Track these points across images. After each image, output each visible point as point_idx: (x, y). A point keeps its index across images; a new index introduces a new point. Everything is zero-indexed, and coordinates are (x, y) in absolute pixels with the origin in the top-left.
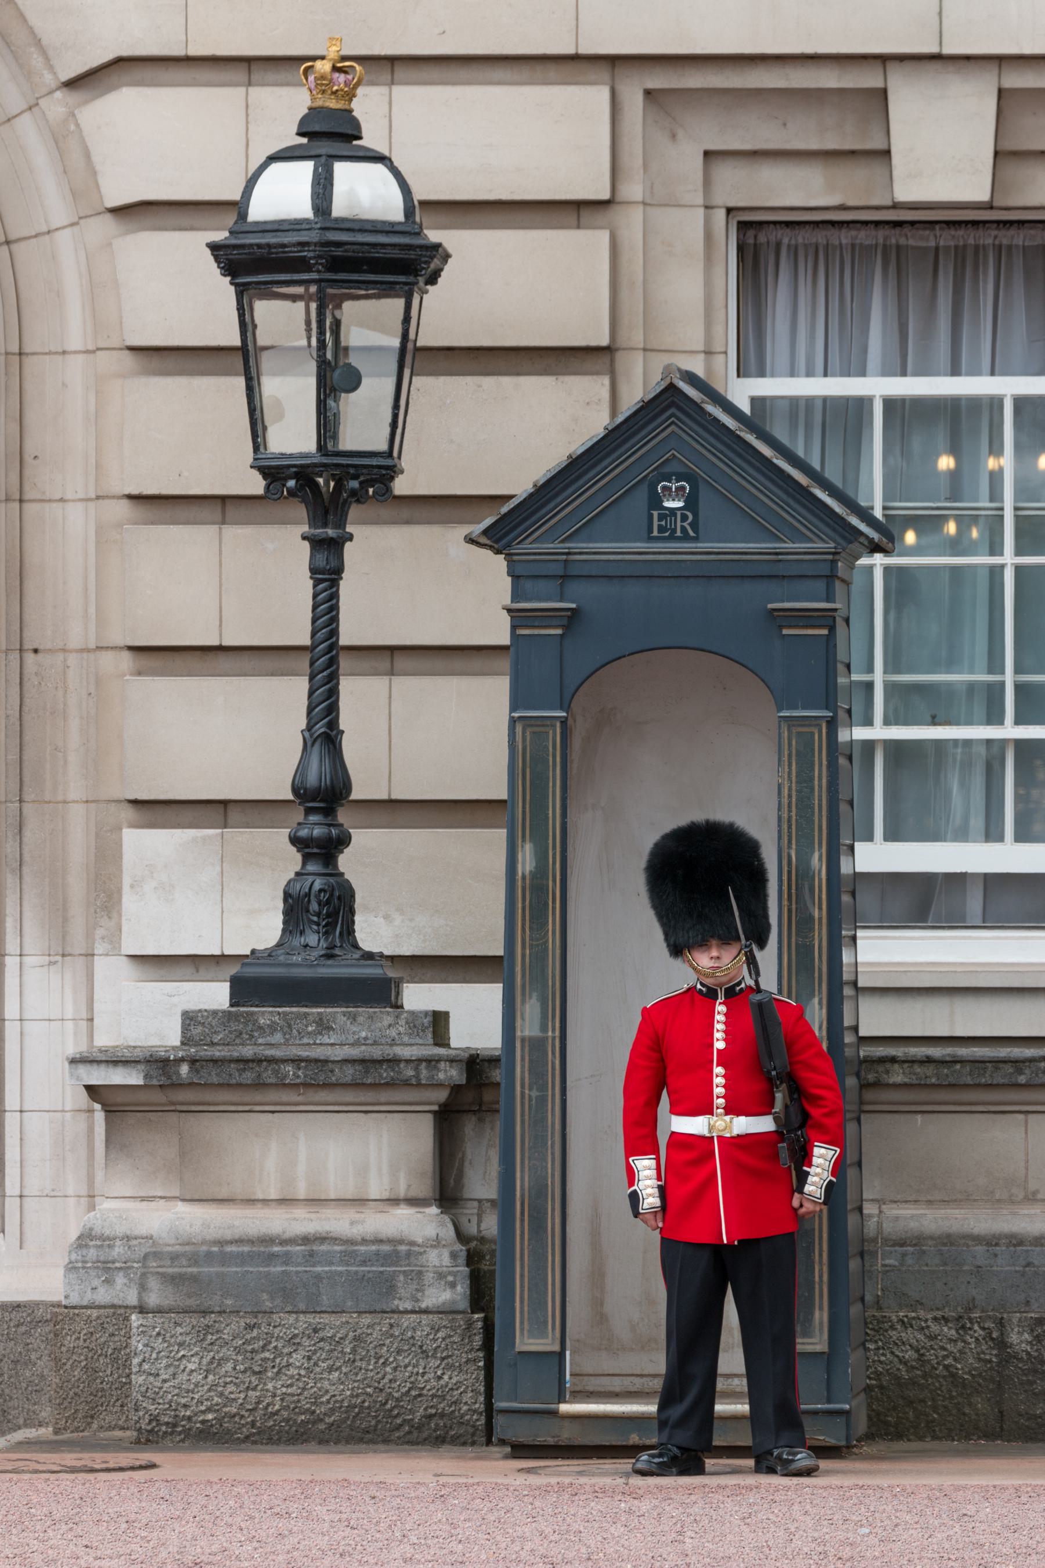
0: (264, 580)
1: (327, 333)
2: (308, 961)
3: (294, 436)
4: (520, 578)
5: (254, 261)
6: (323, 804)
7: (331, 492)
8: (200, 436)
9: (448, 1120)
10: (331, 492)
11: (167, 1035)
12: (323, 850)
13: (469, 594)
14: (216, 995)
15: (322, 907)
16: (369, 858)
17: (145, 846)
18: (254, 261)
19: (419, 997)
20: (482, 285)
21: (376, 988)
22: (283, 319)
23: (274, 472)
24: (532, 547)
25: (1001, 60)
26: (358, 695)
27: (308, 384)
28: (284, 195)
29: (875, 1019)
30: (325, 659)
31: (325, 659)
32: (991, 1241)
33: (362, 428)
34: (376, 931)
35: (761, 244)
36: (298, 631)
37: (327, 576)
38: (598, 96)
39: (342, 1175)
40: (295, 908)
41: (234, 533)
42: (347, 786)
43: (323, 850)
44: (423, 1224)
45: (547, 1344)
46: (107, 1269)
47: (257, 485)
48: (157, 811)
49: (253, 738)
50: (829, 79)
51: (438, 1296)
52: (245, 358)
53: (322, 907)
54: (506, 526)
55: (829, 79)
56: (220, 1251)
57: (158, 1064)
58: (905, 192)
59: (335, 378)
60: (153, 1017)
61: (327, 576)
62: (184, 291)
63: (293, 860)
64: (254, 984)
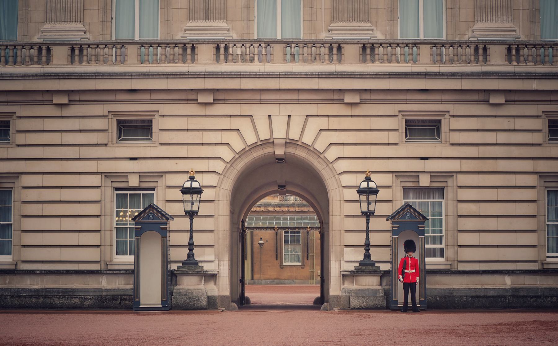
0: (361, 223)
1: (368, 198)
2: (367, 261)
3: (365, 209)
4: (393, 223)
5: (361, 192)
6: (367, 246)
7: (368, 215)
8: (355, 209)
9: (381, 277)
10: (368, 215)
11: (353, 269)
12: (367, 250)
13: (387, 225)
14: (358, 265)
15: (367, 256)
16: (372, 251)
17: (347, 250)
18: (361, 192)
19: (377, 265)
20: (382, 194)
21: (373, 263)
22: (364, 198)
23: (363, 213)
24: (394, 220)
25: (430, 172)
26: (371, 235)
27: (366, 204)
28: (364, 185)
29: (427, 267)
30: (368, 231)
31: (368, 231)
32: (435, 289)
33: (371, 208)
34: (373, 258)
35: (406, 190)
36: (365, 228)
37: (368, 223)
38: (391, 175)
39: (370, 282)
40: (365, 256)
41: (355, 219)
42: (370, 244)
43: (367, 250)
44: (379, 287)
45: (396, 299)
46: (345, 292)
47: (361, 214)
48: (347, 246)
49: (361, 239)
50: (413, 174)
51: (381, 295)
52: (359, 201)
53: (367, 256)
54: (389, 218)
55: (413, 174)
56: (359, 290)
57: (353, 271)
58: (421, 185)
59: (369, 203)
60: (352, 267)
61: (368, 223)
62: (353, 194)
63: (365, 251)
64: (361, 263)
